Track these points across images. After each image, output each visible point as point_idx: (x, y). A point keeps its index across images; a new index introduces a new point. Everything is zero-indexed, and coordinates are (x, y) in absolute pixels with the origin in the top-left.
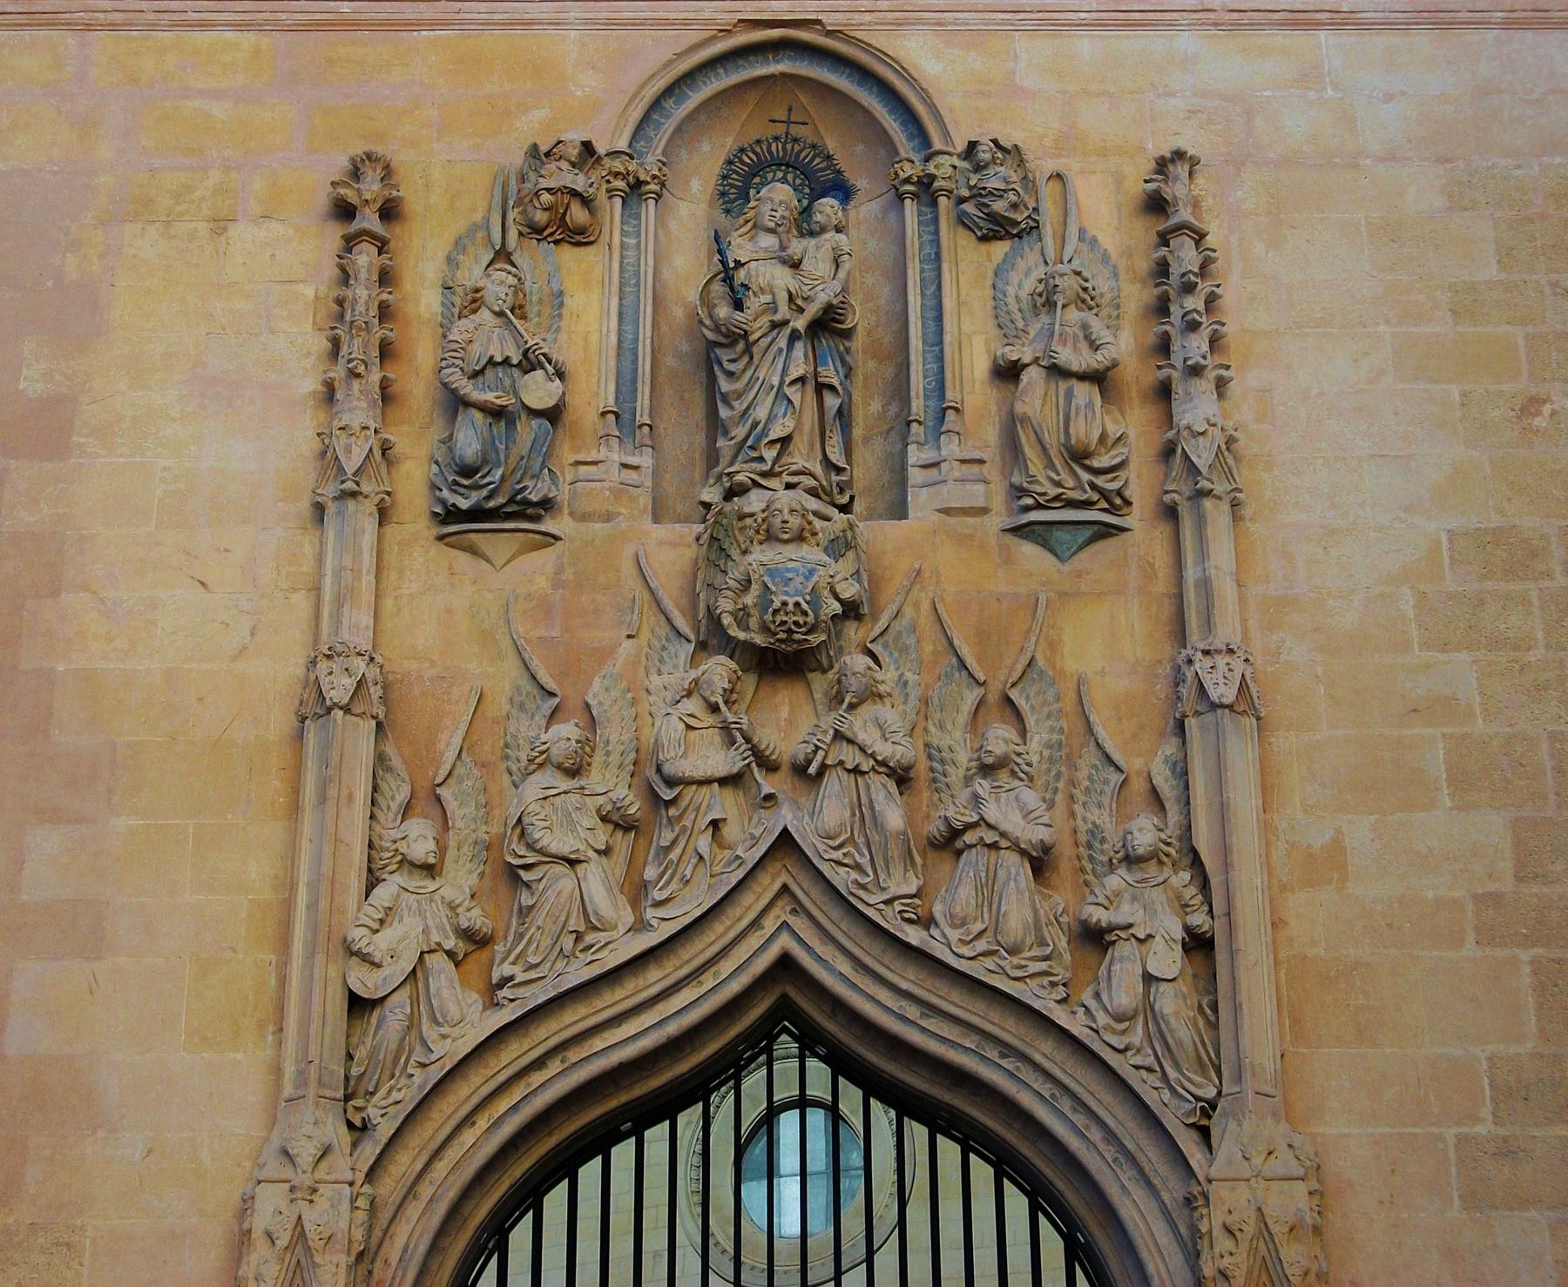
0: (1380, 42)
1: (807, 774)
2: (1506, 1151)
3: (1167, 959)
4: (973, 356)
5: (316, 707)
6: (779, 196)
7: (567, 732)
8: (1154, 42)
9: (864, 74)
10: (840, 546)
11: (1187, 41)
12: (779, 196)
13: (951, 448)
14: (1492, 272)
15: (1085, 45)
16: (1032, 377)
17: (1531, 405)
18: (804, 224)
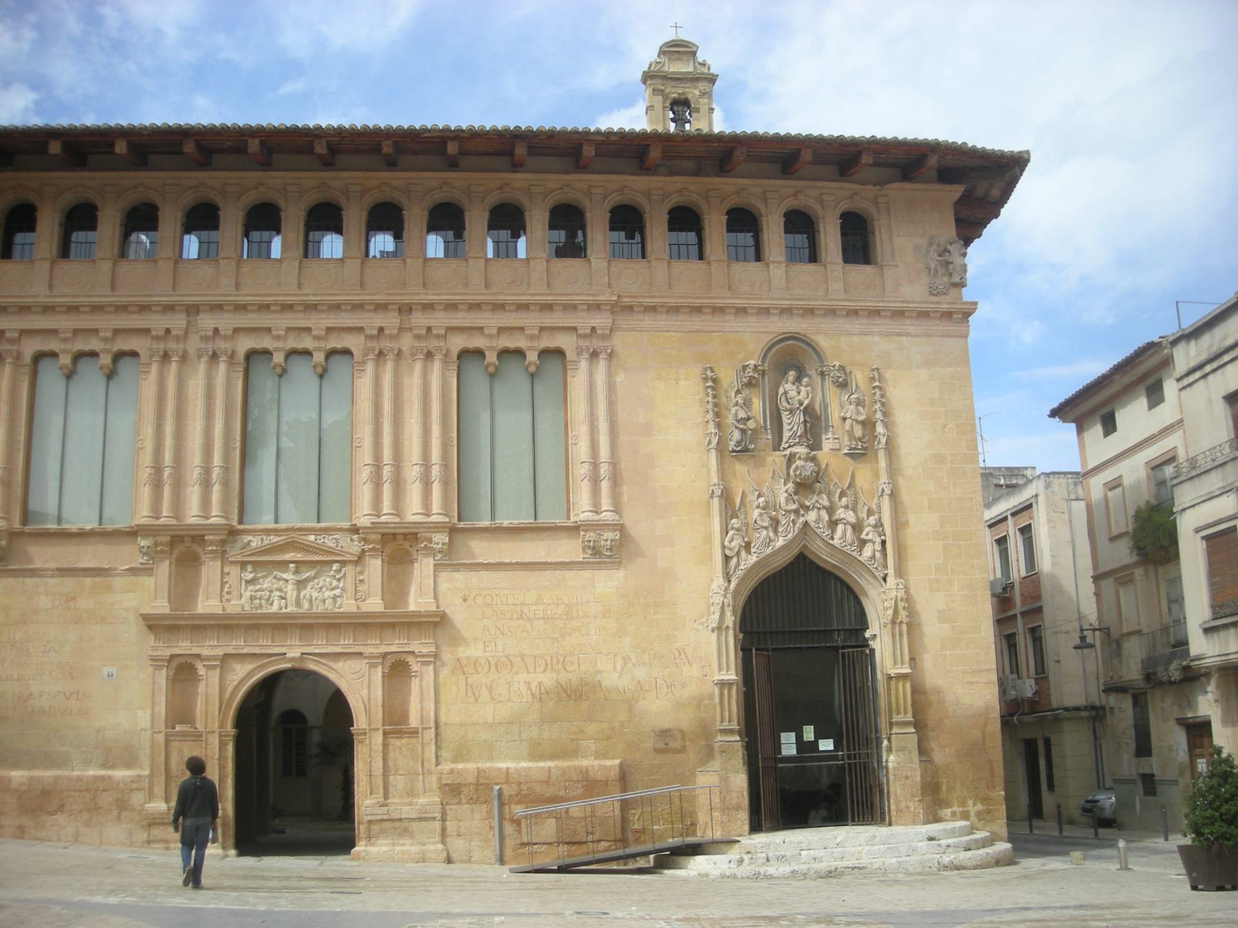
0: (915, 339)
1: (807, 508)
2: (937, 581)
3: (878, 547)
4: (835, 415)
5: (712, 495)
6: (792, 375)
7: (761, 500)
8: (869, 338)
9: (804, 341)
10: (813, 459)
11: (877, 338)
12: (792, 375)
13: (830, 435)
14: (937, 396)
15: (856, 339)
16: (848, 422)
17: (945, 425)
18: (798, 380)
